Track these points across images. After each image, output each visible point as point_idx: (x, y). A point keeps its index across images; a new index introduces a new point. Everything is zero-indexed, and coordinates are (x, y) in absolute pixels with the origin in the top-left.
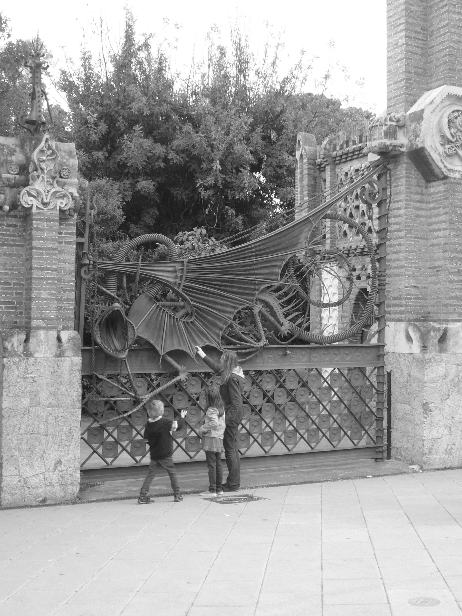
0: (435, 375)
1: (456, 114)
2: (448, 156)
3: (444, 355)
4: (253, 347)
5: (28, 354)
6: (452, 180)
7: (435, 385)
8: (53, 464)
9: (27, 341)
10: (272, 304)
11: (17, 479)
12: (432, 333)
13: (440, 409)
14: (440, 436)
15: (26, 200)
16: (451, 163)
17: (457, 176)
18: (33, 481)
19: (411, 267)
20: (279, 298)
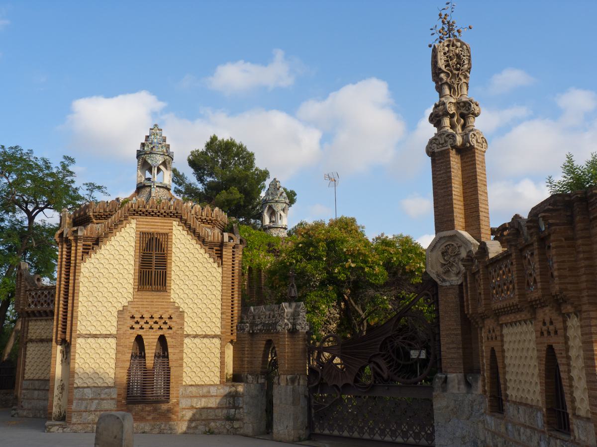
0: (440, 405)
1: (448, 247)
2: (445, 273)
3: (445, 394)
4: (365, 385)
5: (279, 384)
6: (444, 288)
7: (440, 412)
8: (285, 427)
9: (279, 379)
10: (380, 363)
11: (276, 430)
12: (437, 380)
13: (445, 427)
14: (446, 444)
15: (279, 328)
16: (448, 277)
17: (448, 284)
18: (281, 432)
19: (444, 340)
20: (385, 360)
